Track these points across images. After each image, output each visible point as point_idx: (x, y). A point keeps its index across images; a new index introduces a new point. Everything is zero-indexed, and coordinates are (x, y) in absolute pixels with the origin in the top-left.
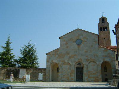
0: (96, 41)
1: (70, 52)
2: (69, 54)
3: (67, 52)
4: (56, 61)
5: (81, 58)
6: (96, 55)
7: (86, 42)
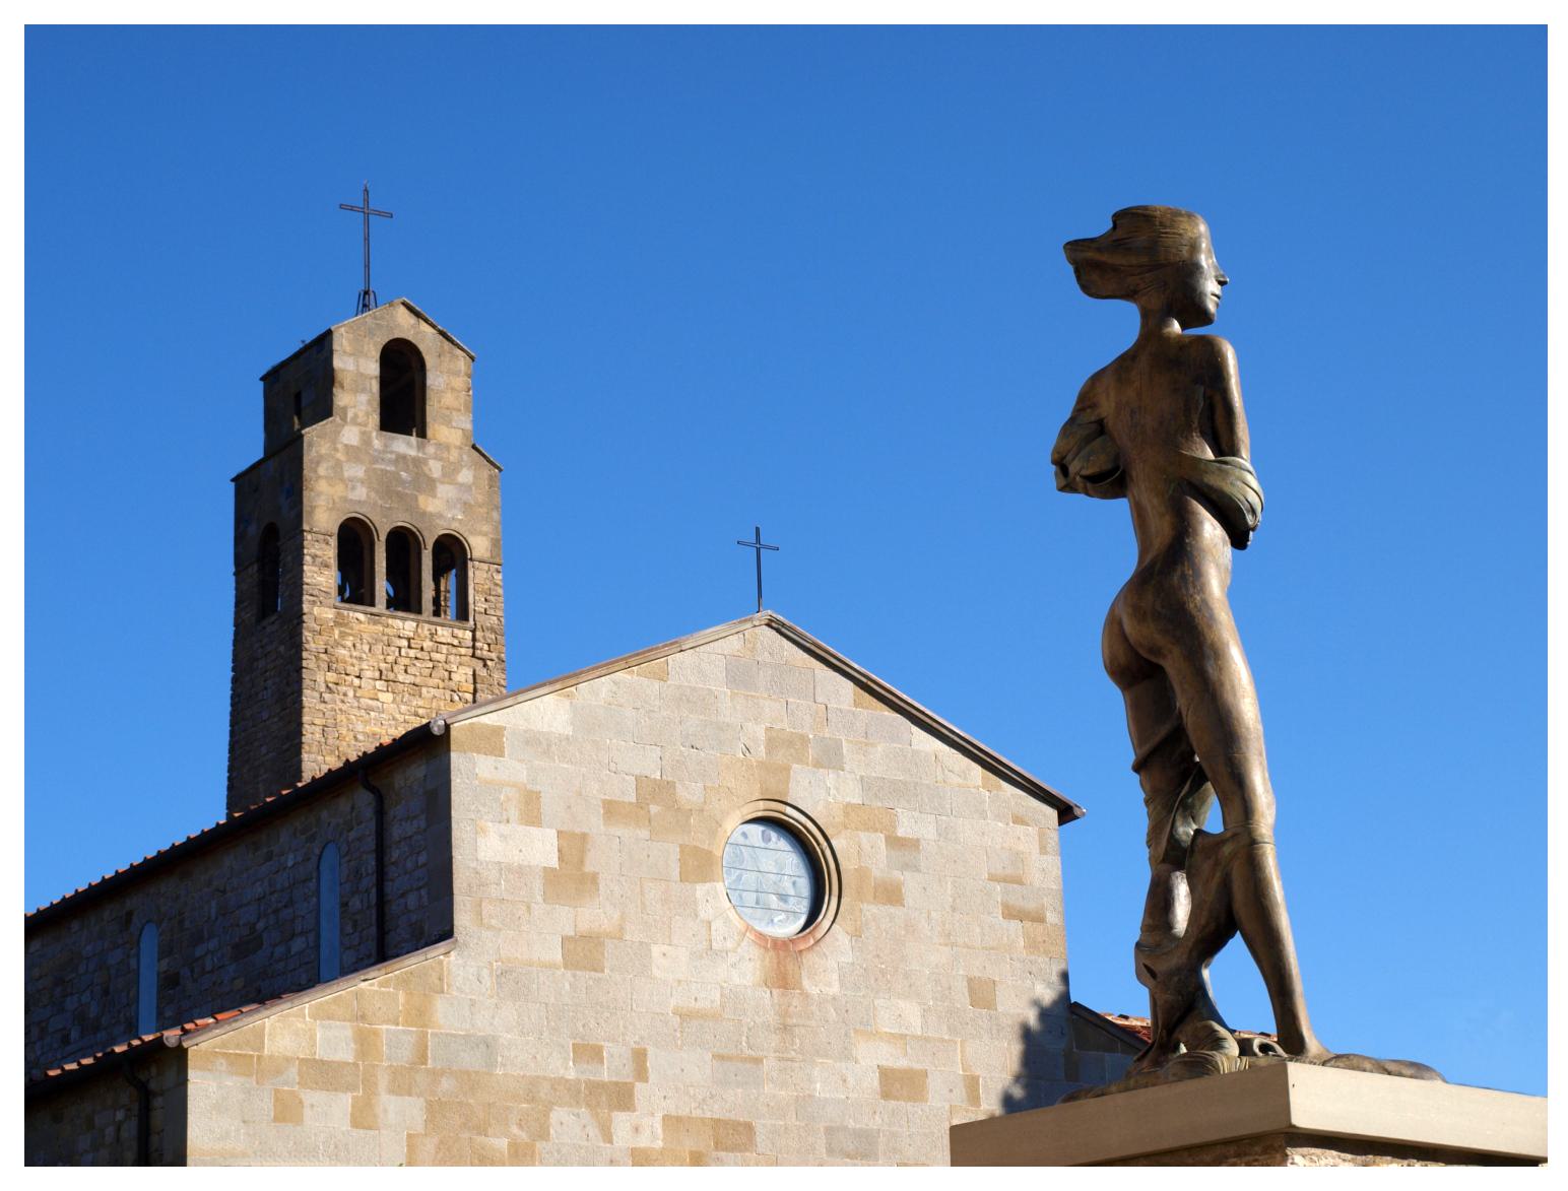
0: (1041, 919)
1: (640, 1057)
2: (622, 1097)
7: (891, 894)
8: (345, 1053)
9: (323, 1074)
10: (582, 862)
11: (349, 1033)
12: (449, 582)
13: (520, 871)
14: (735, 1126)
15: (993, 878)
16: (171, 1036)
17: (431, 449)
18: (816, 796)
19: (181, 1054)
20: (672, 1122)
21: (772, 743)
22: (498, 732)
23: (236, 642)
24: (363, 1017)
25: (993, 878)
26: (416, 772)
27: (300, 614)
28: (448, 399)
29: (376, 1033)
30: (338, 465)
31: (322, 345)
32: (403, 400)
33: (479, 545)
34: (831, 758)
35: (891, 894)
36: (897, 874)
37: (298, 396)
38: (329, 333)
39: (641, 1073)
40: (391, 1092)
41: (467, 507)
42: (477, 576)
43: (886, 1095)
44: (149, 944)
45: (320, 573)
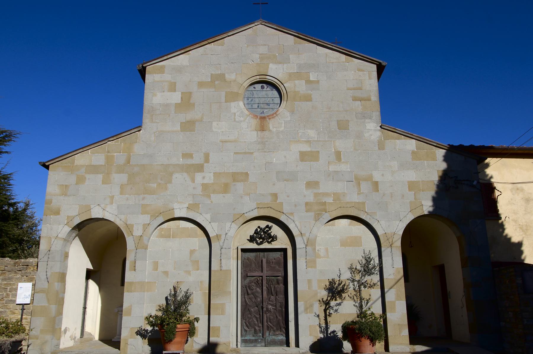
0: (369, 100)
2: (200, 168)
3: (187, 155)
4: (109, 213)
5: (275, 196)
6: (369, 178)
7: (308, 98)
9: (94, 169)
13: (167, 105)
15: (349, 89)
20: (217, 175)
21: (261, 59)
22: (163, 67)
24: (108, 152)
25: (349, 89)
29: (113, 156)
36: (309, 92)
39: (207, 160)
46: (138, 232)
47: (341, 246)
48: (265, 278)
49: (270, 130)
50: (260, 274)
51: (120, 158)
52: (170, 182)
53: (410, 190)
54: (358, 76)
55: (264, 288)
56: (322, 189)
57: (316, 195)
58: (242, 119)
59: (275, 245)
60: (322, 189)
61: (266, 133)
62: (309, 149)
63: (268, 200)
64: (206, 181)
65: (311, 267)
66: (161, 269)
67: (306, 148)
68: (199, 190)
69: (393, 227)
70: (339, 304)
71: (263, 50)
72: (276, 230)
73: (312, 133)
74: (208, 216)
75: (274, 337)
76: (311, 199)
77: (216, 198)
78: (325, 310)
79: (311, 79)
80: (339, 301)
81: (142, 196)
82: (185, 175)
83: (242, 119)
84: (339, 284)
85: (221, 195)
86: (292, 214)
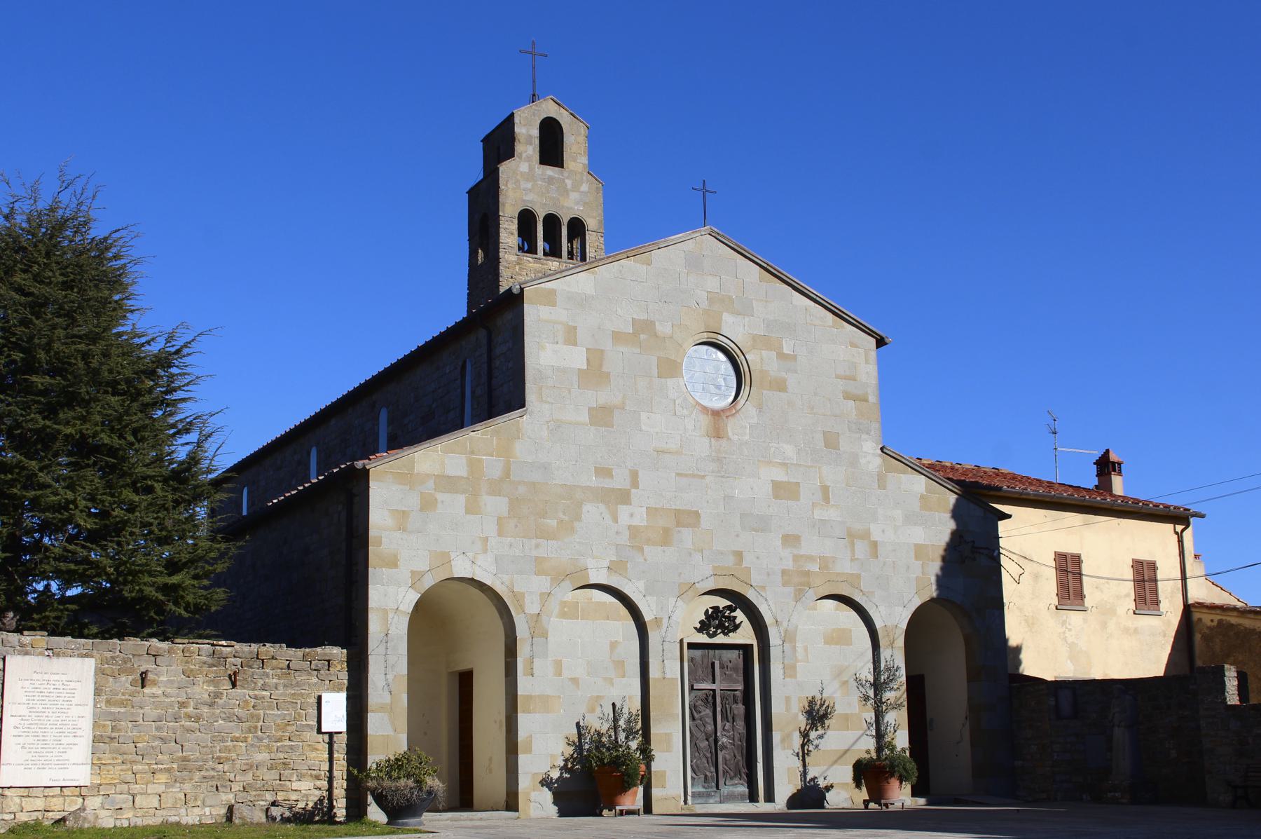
0: (866, 401)
1: (634, 476)
2: (623, 497)
6: (866, 535)
7: (781, 386)
8: (462, 471)
9: (448, 483)
10: (601, 365)
11: (464, 461)
12: (577, 244)
14: (689, 513)
15: (838, 377)
16: (359, 464)
17: (566, 174)
18: (734, 330)
19: (365, 473)
22: (553, 292)
23: (469, 275)
24: (472, 453)
26: (508, 316)
27: (498, 258)
28: (574, 149)
29: (480, 461)
30: (517, 181)
31: (509, 121)
32: (551, 146)
33: (591, 223)
34: (745, 311)
35: (781, 386)
37: (499, 148)
38: (513, 114)
39: (635, 484)
40: (489, 494)
41: (585, 204)
42: (589, 238)
43: (776, 496)
44: (383, 416)
45: (509, 236)
46: (532, 607)
47: (826, 643)
48: (718, 693)
49: (729, 439)
50: (713, 687)
51: (493, 466)
52: (578, 518)
53: (917, 558)
54: (851, 353)
55: (719, 709)
56: (807, 548)
57: (796, 558)
58: (685, 412)
59: (733, 639)
60: (807, 548)
61: (724, 442)
62: (785, 479)
63: (730, 561)
64: (636, 522)
65: (790, 676)
66: (566, 674)
67: (781, 476)
68: (624, 539)
69: (894, 618)
70: (821, 737)
71: (712, 284)
72: (740, 615)
73: (789, 450)
74: (641, 585)
75: (731, 788)
76: (789, 564)
77: (653, 553)
78: (803, 746)
79: (786, 351)
80: (821, 731)
81: (534, 541)
82: (602, 507)
83: (685, 412)
84: (822, 705)
85: (660, 548)
86: (763, 588)
